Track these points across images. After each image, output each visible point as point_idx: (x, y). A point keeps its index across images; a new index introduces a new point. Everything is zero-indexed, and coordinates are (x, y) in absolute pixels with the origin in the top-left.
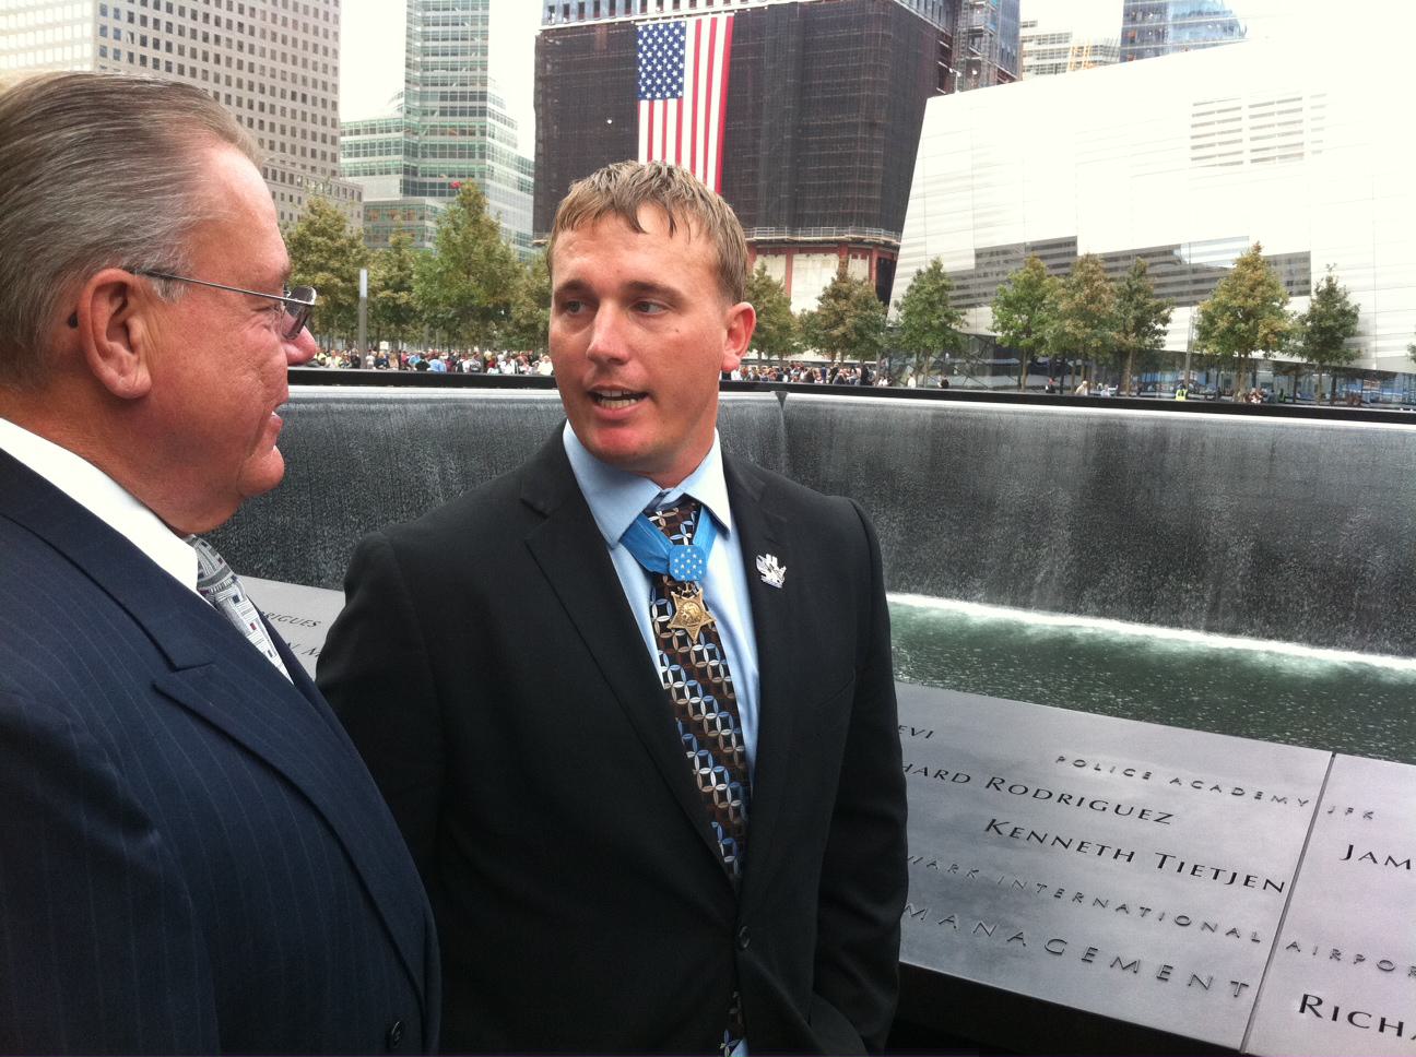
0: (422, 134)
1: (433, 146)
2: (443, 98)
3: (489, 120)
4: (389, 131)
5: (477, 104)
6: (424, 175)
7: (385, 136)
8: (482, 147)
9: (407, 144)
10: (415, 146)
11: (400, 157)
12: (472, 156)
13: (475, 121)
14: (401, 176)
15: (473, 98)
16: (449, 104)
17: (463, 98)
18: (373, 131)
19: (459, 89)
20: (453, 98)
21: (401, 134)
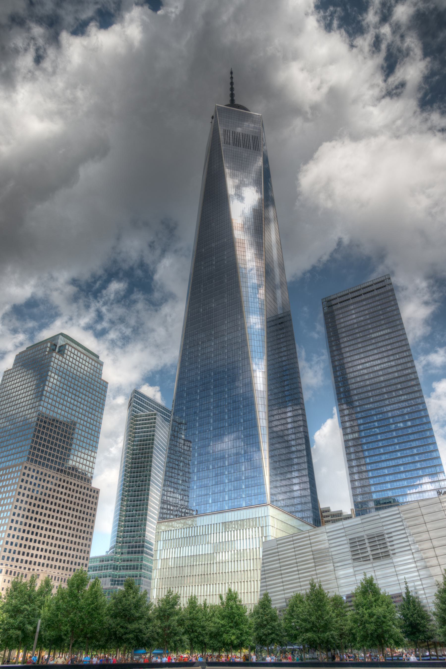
0: (120, 561)
1: (123, 566)
2: (129, 548)
3: (144, 555)
4: (108, 561)
5: (141, 549)
6: (119, 577)
7: (107, 562)
8: (141, 565)
9: (114, 565)
10: (117, 566)
11: (111, 570)
12: (137, 569)
13: (140, 556)
14: (111, 578)
15: (139, 547)
16: (130, 549)
17: (136, 547)
18: (103, 561)
19: (135, 544)
20: (132, 547)
21: (113, 562)
